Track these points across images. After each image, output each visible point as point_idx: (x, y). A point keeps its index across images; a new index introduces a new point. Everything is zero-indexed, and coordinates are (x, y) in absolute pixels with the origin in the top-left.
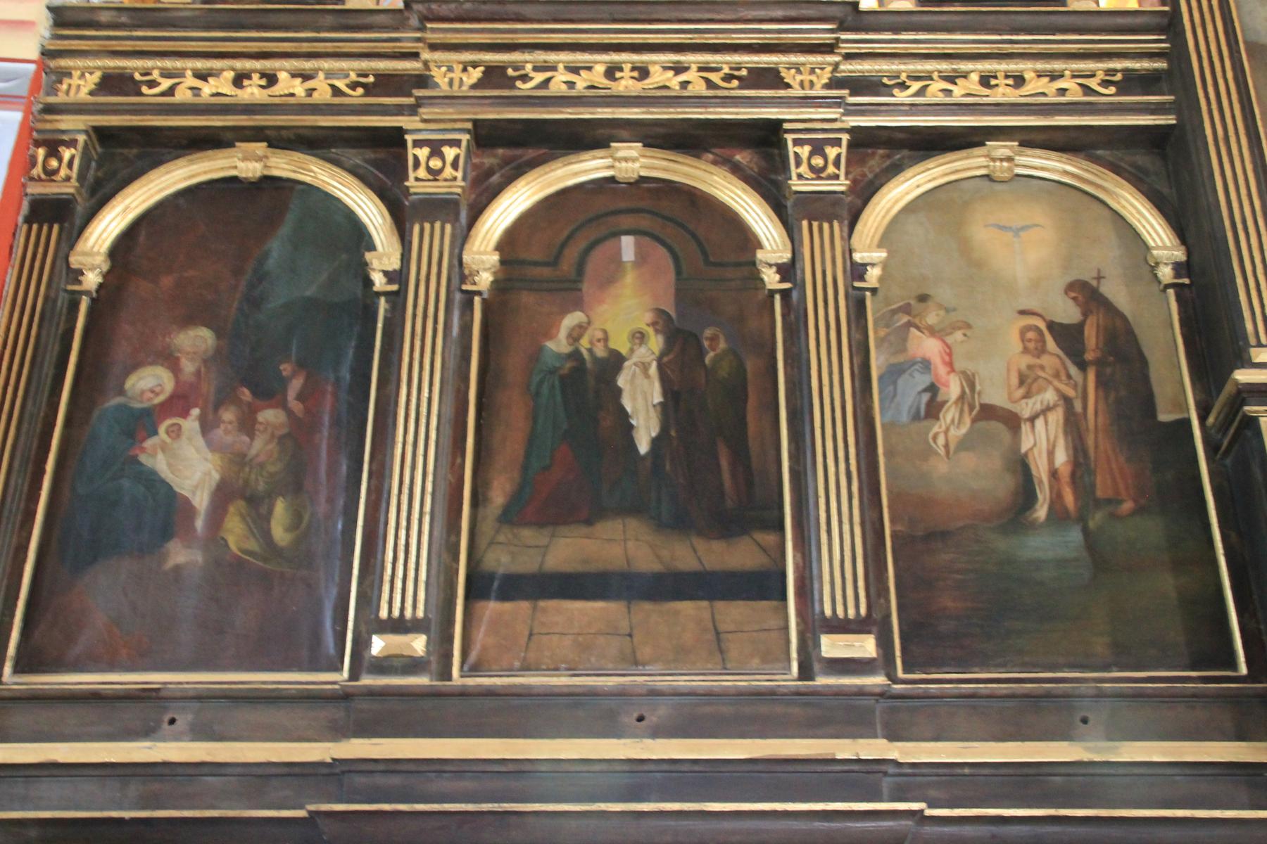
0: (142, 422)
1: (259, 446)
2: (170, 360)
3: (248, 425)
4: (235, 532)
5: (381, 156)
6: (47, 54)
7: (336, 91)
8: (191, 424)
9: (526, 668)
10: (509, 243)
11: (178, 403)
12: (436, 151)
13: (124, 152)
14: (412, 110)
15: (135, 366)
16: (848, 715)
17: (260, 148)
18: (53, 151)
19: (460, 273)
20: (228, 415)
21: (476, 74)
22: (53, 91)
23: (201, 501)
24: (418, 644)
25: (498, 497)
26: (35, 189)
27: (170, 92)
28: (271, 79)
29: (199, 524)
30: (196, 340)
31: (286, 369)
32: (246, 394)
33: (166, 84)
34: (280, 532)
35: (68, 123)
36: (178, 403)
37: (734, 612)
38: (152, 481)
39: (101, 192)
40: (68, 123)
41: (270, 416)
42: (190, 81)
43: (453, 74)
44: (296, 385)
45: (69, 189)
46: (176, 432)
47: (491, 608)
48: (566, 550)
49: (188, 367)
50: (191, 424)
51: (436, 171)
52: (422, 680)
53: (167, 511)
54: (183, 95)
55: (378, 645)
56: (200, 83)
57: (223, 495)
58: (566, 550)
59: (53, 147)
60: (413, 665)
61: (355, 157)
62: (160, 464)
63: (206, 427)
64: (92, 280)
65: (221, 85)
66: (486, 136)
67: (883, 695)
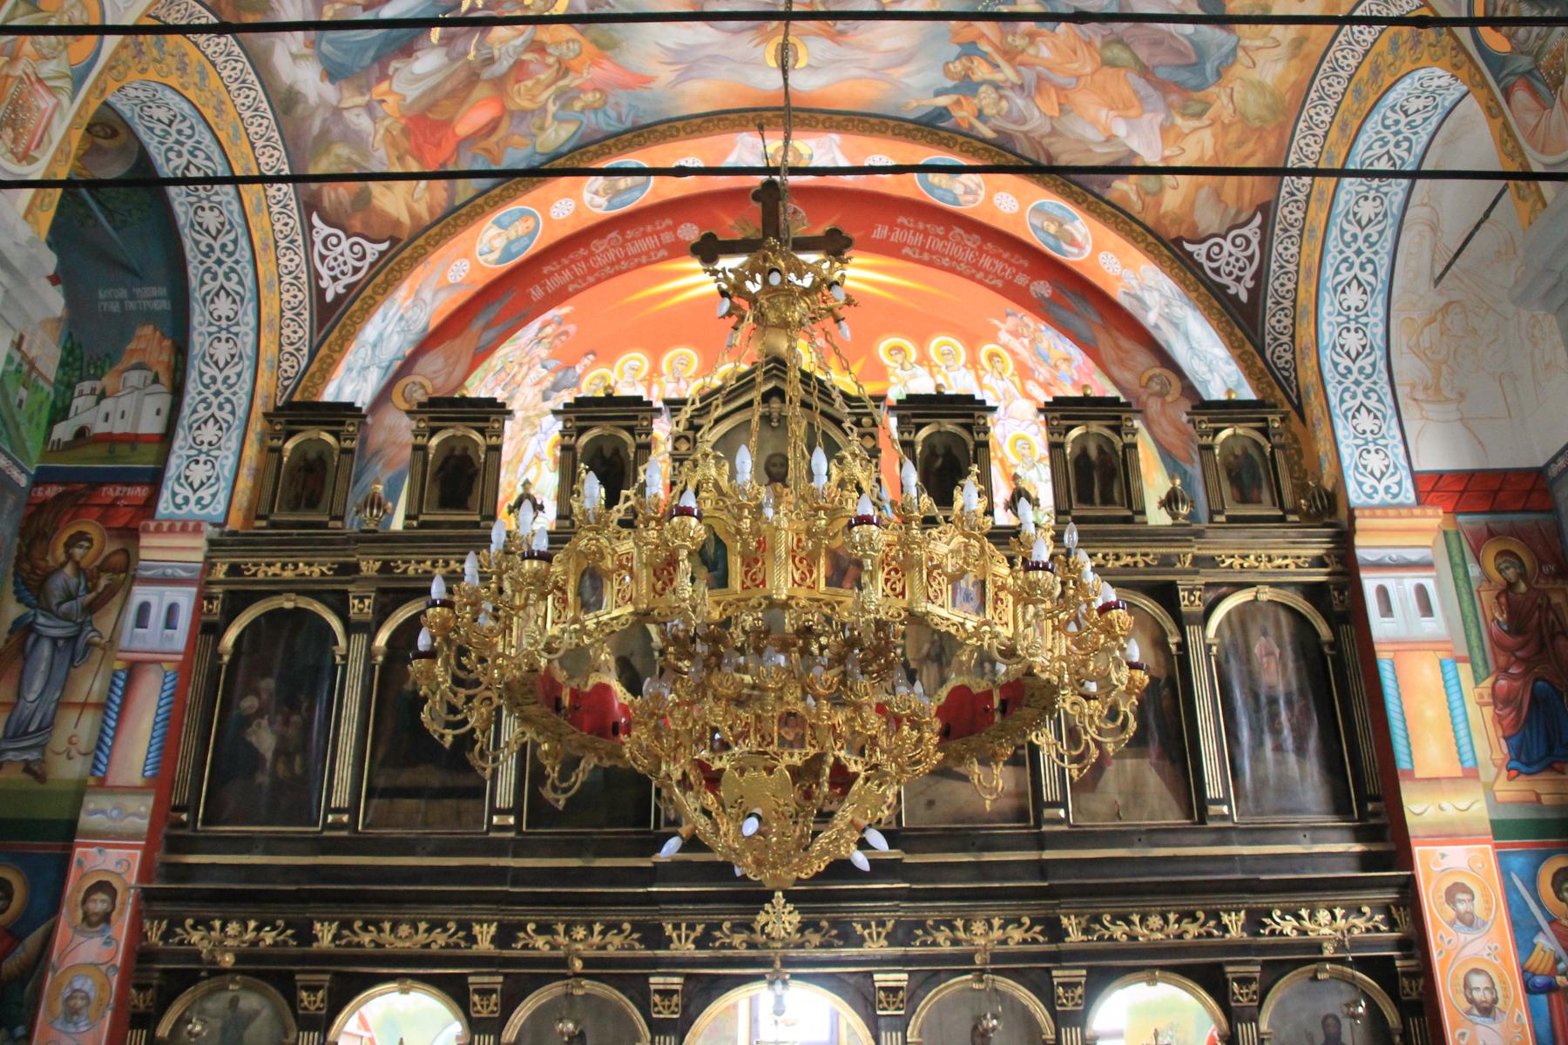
0: (246, 721)
1: (292, 732)
2: (257, 693)
3: (286, 722)
4: (281, 769)
5: (340, 605)
6: (207, 558)
7: (323, 574)
8: (265, 722)
9: (387, 826)
10: (389, 643)
11: (260, 713)
12: (361, 601)
13: (237, 602)
14: (352, 582)
15: (243, 696)
16: (499, 848)
17: (293, 596)
18: (210, 602)
19: (370, 654)
20: (279, 718)
21: (378, 564)
22: (210, 574)
23: (269, 755)
24: (345, 818)
25: (380, 755)
26: (204, 618)
27: (255, 574)
28: (296, 566)
29: (268, 765)
30: (268, 684)
31: (302, 697)
32: (286, 709)
33: (253, 569)
34: (298, 769)
35: (217, 589)
36: (260, 713)
37: (468, 804)
38: (249, 745)
39: (230, 615)
40: (217, 589)
41: (295, 718)
42: (263, 568)
43: (369, 567)
44: (305, 705)
45: (216, 618)
46: (259, 726)
47: (375, 802)
48: (406, 778)
49: (264, 696)
50: (265, 722)
51: (362, 608)
52: (344, 833)
53: (255, 757)
54: (261, 576)
55: (330, 818)
56: (267, 569)
57: (278, 752)
58: (406, 778)
59: (210, 599)
60: (342, 826)
61: (331, 599)
62: (253, 739)
63: (271, 723)
64: (226, 658)
65: (276, 569)
66: (382, 592)
67: (512, 839)
